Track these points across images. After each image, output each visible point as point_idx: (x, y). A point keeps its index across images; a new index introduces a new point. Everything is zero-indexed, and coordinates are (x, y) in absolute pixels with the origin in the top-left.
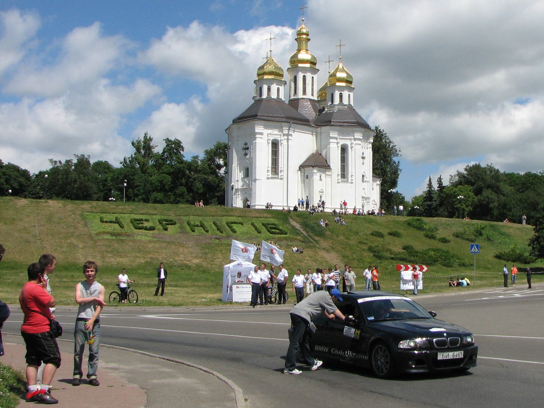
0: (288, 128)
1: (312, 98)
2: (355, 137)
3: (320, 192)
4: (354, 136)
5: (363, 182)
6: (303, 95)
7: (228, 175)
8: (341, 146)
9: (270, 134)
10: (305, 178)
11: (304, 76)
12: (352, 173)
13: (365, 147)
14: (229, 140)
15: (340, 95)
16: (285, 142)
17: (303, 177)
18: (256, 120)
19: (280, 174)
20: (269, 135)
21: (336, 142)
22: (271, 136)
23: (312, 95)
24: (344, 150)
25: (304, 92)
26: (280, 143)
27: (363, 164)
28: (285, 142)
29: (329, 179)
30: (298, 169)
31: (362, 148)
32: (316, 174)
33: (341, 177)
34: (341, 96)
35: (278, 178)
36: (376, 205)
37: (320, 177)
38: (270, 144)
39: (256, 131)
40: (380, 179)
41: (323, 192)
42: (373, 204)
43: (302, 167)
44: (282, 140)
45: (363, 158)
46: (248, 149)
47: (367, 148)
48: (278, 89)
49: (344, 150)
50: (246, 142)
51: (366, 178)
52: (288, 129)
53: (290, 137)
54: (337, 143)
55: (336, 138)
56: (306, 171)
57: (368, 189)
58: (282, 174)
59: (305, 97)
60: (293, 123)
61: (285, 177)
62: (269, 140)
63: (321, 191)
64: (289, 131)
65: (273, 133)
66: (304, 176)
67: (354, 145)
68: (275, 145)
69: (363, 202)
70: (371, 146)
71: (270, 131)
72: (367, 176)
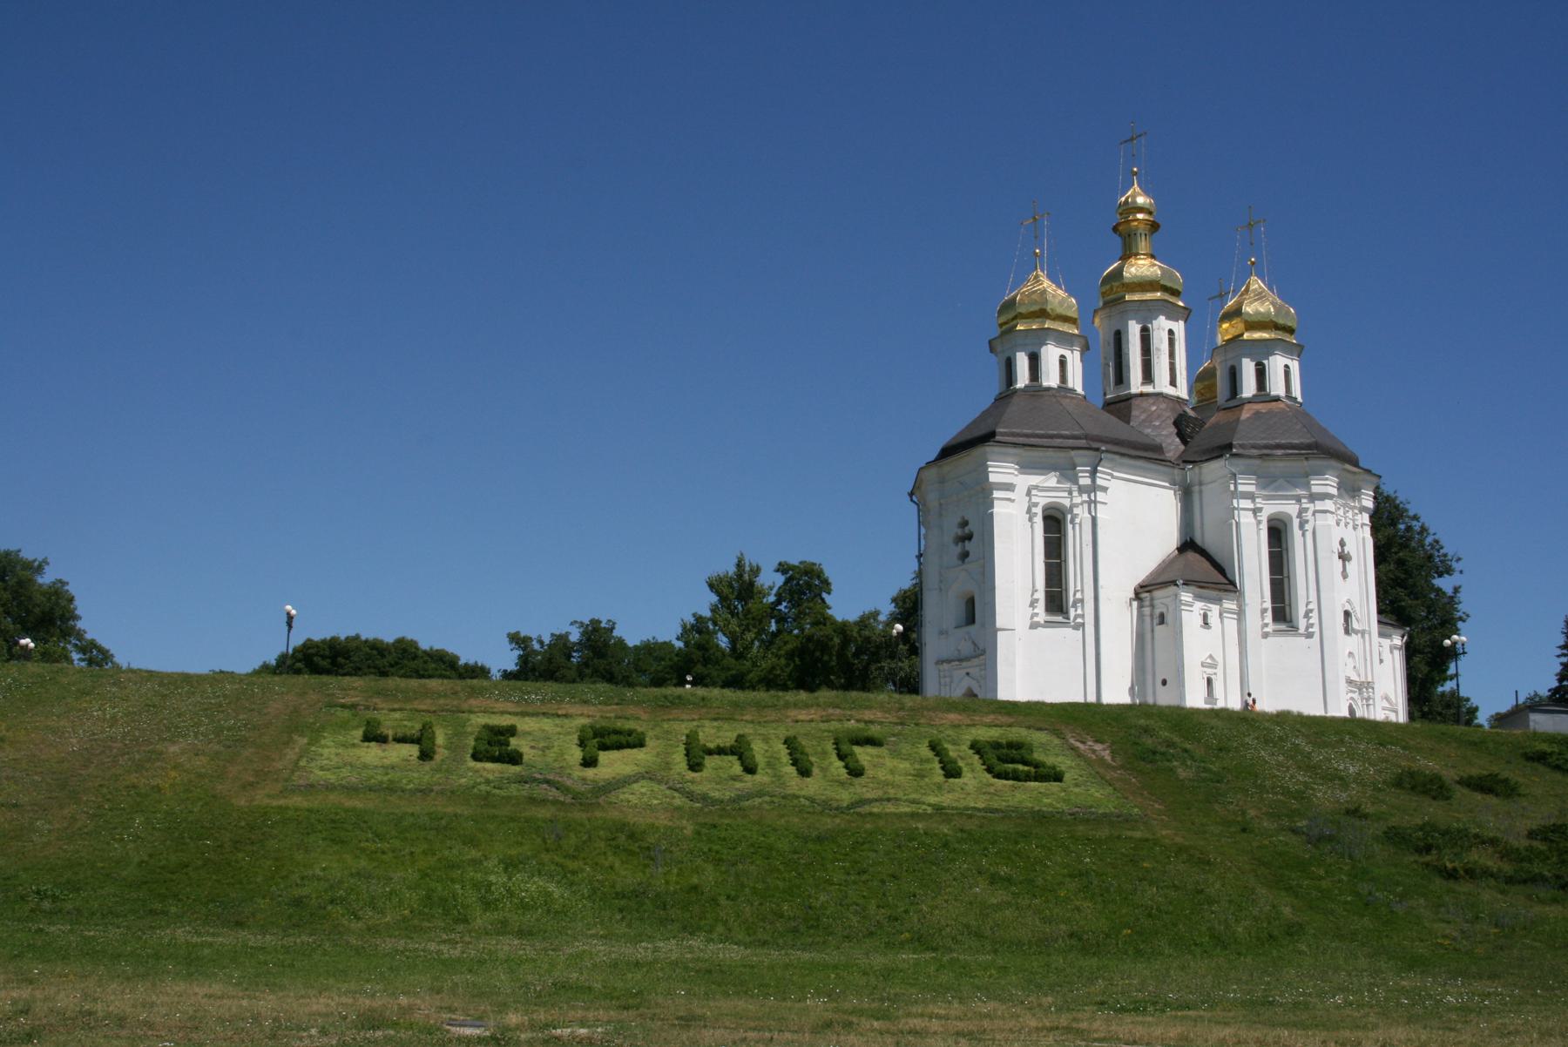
1: (1170, 391)
2: (1315, 489)
4: (1308, 486)
5: (1347, 631)
6: (1143, 384)
8: (1270, 520)
9: (1036, 487)
10: (1156, 621)
14: (919, 522)
16: (1082, 513)
19: (1072, 613)
20: (1034, 492)
21: (1252, 506)
22: (1040, 494)
23: (1173, 383)
25: (1148, 376)
27: (1345, 575)
30: (1133, 596)
31: (1338, 524)
32: (1191, 609)
37: (1205, 617)
39: (993, 478)
40: (1401, 632)
41: (1214, 666)
42: (1384, 709)
43: (1143, 591)
44: (1077, 505)
46: (969, 537)
48: (1063, 362)
49: (1278, 534)
50: (963, 518)
53: (1100, 496)
54: (1256, 511)
56: (1156, 602)
58: (1079, 612)
59: (1148, 389)
60: (1107, 451)
62: (1036, 505)
63: (1209, 661)
66: (1152, 616)
69: (1352, 698)
70: (1366, 518)
71: (1035, 480)
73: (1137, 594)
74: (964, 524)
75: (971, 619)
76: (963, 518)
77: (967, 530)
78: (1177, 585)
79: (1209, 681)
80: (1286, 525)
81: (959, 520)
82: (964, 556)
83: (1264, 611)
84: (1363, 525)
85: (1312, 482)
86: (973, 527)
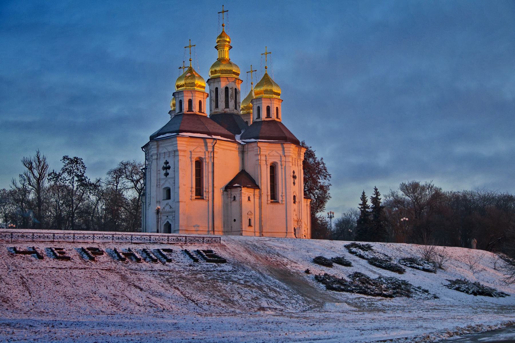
7: (146, 197)
10: (232, 199)
25: (227, 106)
27: (294, 183)
35: (203, 199)
37: (249, 197)
38: (194, 163)
45: (294, 177)
46: (169, 168)
50: (166, 161)
57: (299, 211)
59: (227, 110)
67: (283, 163)
74: (167, 163)
75: (169, 197)
76: (166, 161)
77: (168, 165)
78: (241, 188)
81: (165, 161)
82: (167, 174)
86: (171, 164)
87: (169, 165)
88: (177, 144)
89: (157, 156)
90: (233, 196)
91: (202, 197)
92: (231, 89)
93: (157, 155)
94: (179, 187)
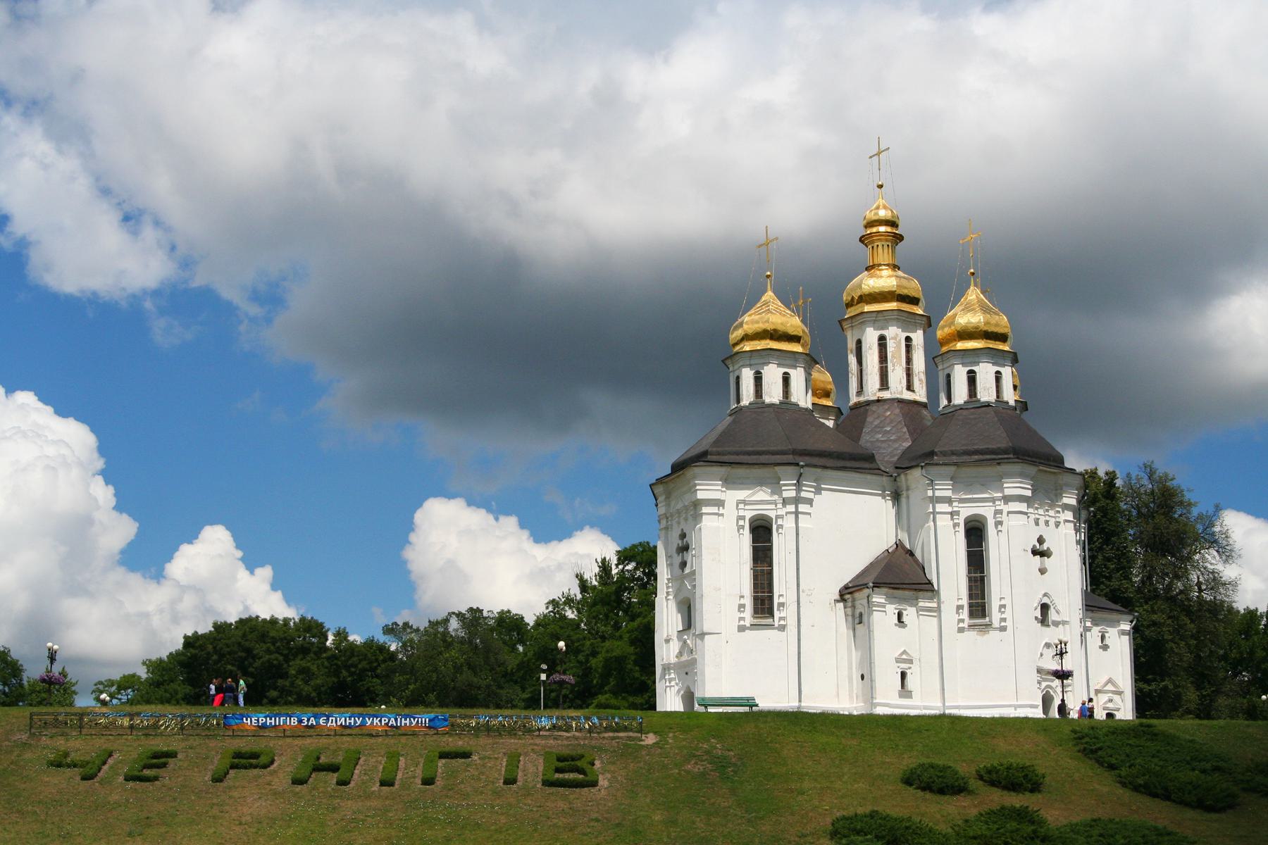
0: (795, 482)
1: (908, 396)
2: (1008, 492)
3: (898, 660)
4: (1002, 489)
9: (744, 502)
10: (857, 621)
11: (882, 339)
12: (1001, 599)
13: (1047, 523)
15: (969, 377)
16: (789, 523)
17: (850, 619)
18: (701, 463)
19: (777, 614)
20: (741, 506)
21: (950, 509)
23: (910, 387)
24: (975, 533)
26: (774, 527)
28: (789, 523)
29: (930, 623)
30: (838, 597)
31: (1037, 524)
33: (972, 614)
34: (972, 379)
35: (771, 626)
36: (1120, 693)
37: (900, 616)
40: (1131, 617)
41: (911, 662)
44: (781, 517)
47: (1057, 524)
48: (786, 379)
49: (975, 533)
50: (682, 530)
51: (1058, 612)
52: (795, 485)
53: (802, 508)
54: (953, 514)
55: (949, 501)
56: (857, 603)
59: (886, 395)
60: (807, 465)
61: (791, 622)
62: (743, 518)
63: (904, 657)
64: (799, 490)
65: (754, 498)
66: (853, 616)
67: (1004, 517)
68: (761, 532)
70: (1069, 515)
71: (742, 494)
72: (1059, 607)
73: (841, 595)
76: (682, 530)
77: (685, 540)
79: (903, 675)
80: (984, 527)
83: (960, 607)
84: (1066, 521)
85: (1005, 485)
87: (687, 542)
88: (696, 485)
89: (667, 522)
90: (857, 614)
91: (769, 621)
92: (892, 338)
93: (667, 518)
94: (702, 595)
